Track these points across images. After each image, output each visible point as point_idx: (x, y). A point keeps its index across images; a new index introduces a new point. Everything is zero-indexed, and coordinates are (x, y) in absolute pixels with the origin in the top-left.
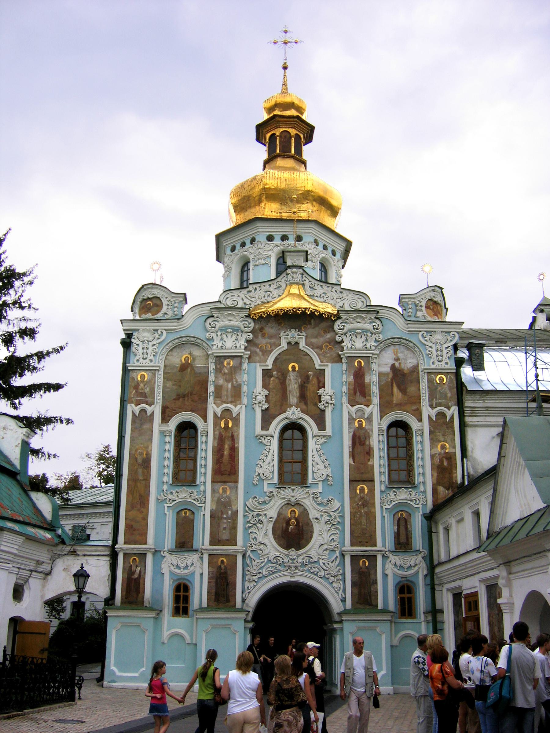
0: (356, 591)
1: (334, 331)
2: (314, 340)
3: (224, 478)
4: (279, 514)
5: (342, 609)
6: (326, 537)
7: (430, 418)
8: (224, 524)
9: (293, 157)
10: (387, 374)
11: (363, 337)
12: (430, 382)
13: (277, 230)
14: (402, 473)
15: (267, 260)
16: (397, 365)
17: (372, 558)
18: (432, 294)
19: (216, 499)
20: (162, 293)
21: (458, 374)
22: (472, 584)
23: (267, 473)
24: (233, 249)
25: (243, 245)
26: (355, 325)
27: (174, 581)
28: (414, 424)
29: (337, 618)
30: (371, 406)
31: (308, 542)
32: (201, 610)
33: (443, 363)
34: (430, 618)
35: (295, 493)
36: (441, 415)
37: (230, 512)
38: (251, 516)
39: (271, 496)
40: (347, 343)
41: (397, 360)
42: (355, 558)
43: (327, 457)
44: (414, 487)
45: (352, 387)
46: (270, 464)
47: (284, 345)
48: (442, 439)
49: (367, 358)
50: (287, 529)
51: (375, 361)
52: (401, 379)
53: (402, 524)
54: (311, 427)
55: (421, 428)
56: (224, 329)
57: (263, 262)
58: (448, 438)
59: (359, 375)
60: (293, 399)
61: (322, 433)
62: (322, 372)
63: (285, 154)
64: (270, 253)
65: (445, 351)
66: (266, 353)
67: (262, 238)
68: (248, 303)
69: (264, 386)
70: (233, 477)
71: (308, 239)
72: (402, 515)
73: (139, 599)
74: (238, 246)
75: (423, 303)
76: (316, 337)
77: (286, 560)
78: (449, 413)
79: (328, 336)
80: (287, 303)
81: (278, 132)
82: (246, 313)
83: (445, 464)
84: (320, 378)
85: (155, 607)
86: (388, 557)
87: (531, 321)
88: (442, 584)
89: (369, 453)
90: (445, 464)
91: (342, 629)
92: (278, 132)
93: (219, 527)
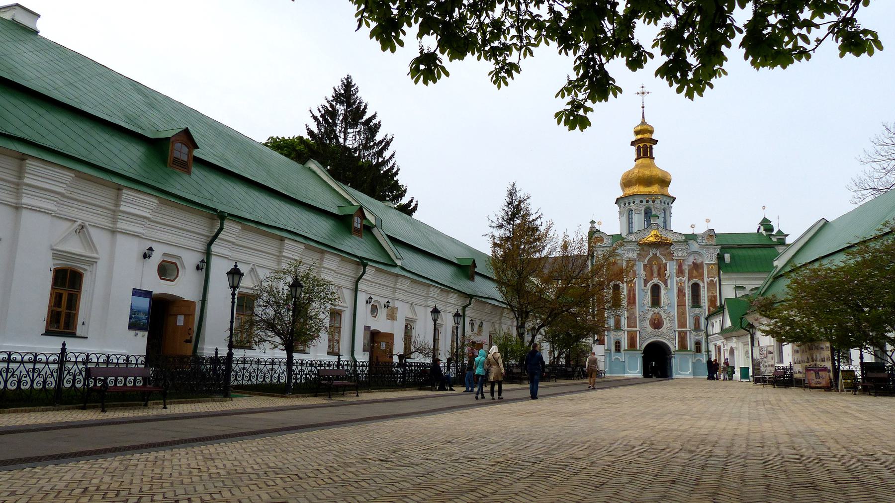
22: (719, 343)
25: (629, 203)
28: (701, 284)
35: (656, 310)
36: (712, 281)
40: (675, 254)
42: (679, 333)
43: (668, 297)
46: (648, 299)
47: (651, 255)
52: (697, 267)
54: (662, 286)
56: (628, 250)
60: (655, 275)
63: (645, 156)
71: (657, 201)
80: (652, 239)
81: (641, 145)
89: (684, 295)
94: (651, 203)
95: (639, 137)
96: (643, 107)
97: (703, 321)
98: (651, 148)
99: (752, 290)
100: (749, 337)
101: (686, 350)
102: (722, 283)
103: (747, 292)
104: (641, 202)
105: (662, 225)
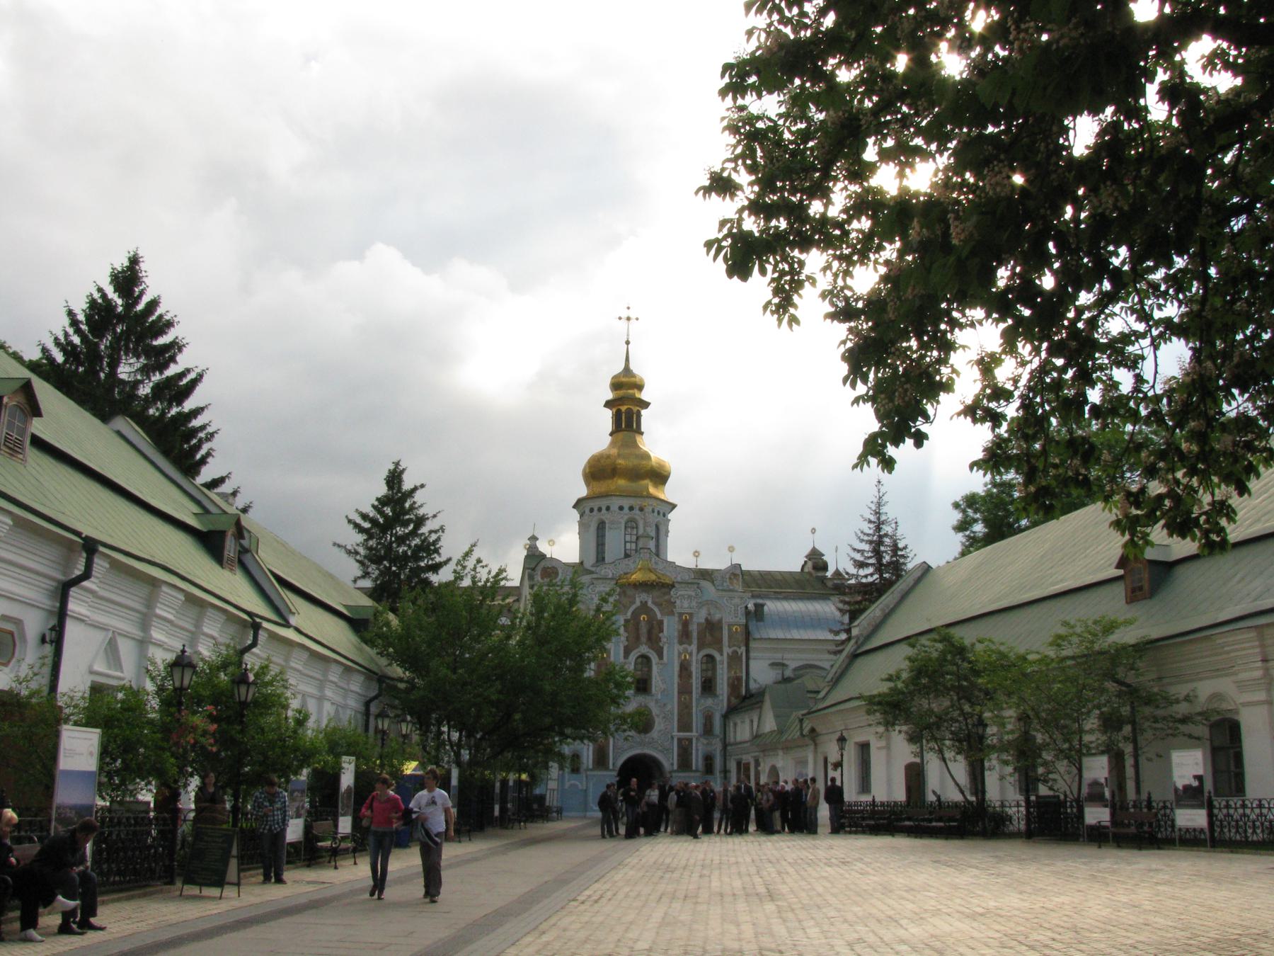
6: (662, 727)
12: (730, 630)
13: (626, 503)
14: (708, 686)
17: (690, 740)
21: (746, 626)
22: (748, 758)
24: (592, 510)
25: (600, 510)
28: (718, 657)
32: (588, 769)
40: (678, 602)
42: (680, 740)
47: (638, 603)
49: (691, 615)
52: (712, 628)
53: (708, 719)
55: (722, 660)
59: (685, 624)
60: (644, 639)
62: (661, 622)
66: (626, 608)
67: (614, 508)
69: (626, 630)
89: (690, 676)
92: (624, 408)
94: (636, 511)
95: (621, 393)
96: (628, 343)
98: (639, 415)
99: (795, 670)
100: (812, 747)
102: (752, 654)
103: (788, 673)
104: (621, 508)
105: (654, 550)
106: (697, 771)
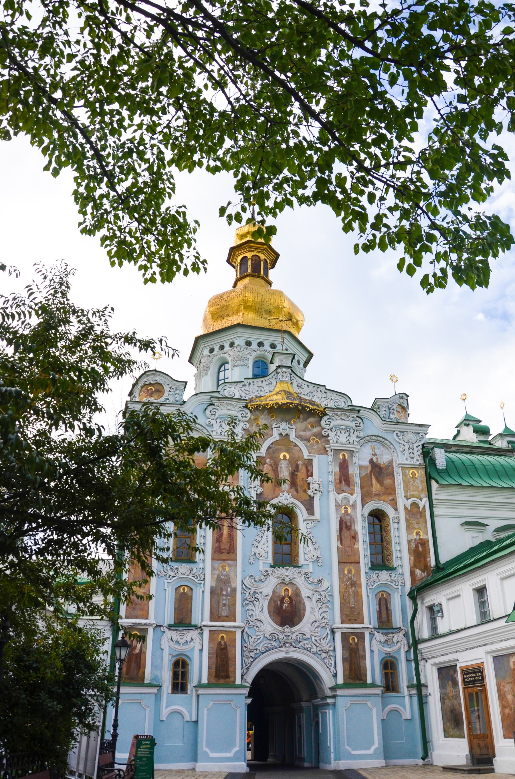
0: (347, 667)
1: (320, 426)
2: (302, 433)
3: (224, 556)
4: (274, 592)
5: (334, 684)
6: (317, 615)
7: (406, 508)
8: (224, 601)
9: (262, 278)
10: (367, 467)
11: (347, 434)
12: (404, 474)
13: (255, 337)
15: (246, 362)
16: (375, 459)
17: (361, 636)
18: (401, 401)
19: (216, 576)
20: (164, 380)
23: (263, 553)
24: (212, 351)
25: (222, 348)
26: (340, 422)
27: (173, 656)
29: (329, 693)
30: (355, 495)
31: (300, 620)
32: (200, 686)
33: (415, 460)
34: (414, 692)
36: (415, 505)
37: (229, 589)
38: (247, 594)
39: (266, 575)
40: (332, 436)
41: (375, 455)
42: (345, 636)
44: (394, 569)
45: (338, 477)
47: (276, 437)
48: (416, 526)
50: (281, 606)
51: (357, 454)
52: (379, 471)
54: (301, 512)
57: (242, 363)
58: (422, 526)
59: (344, 466)
61: (311, 517)
64: (248, 356)
65: (416, 450)
67: (240, 342)
68: (243, 395)
70: (232, 556)
72: (382, 595)
73: (140, 675)
74: (216, 349)
75: (395, 407)
76: (304, 431)
77: (281, 637)
78: (421, 504)
79: (316, 430)
81: (249, 255)
82: (244, 404)
83: (420, 549)
84: (309, 468)
85: (154, 683)
86: (374, 635)
87: (456, 433)
88: (426, 660)
89: (354, 537)
90: (420, 549)
91: (334, 704)
93: (219, 602)
97: (399, 604)
101: (364, 684)
102: (436, 511)
104: (248, 344)
106: (373, 685)
